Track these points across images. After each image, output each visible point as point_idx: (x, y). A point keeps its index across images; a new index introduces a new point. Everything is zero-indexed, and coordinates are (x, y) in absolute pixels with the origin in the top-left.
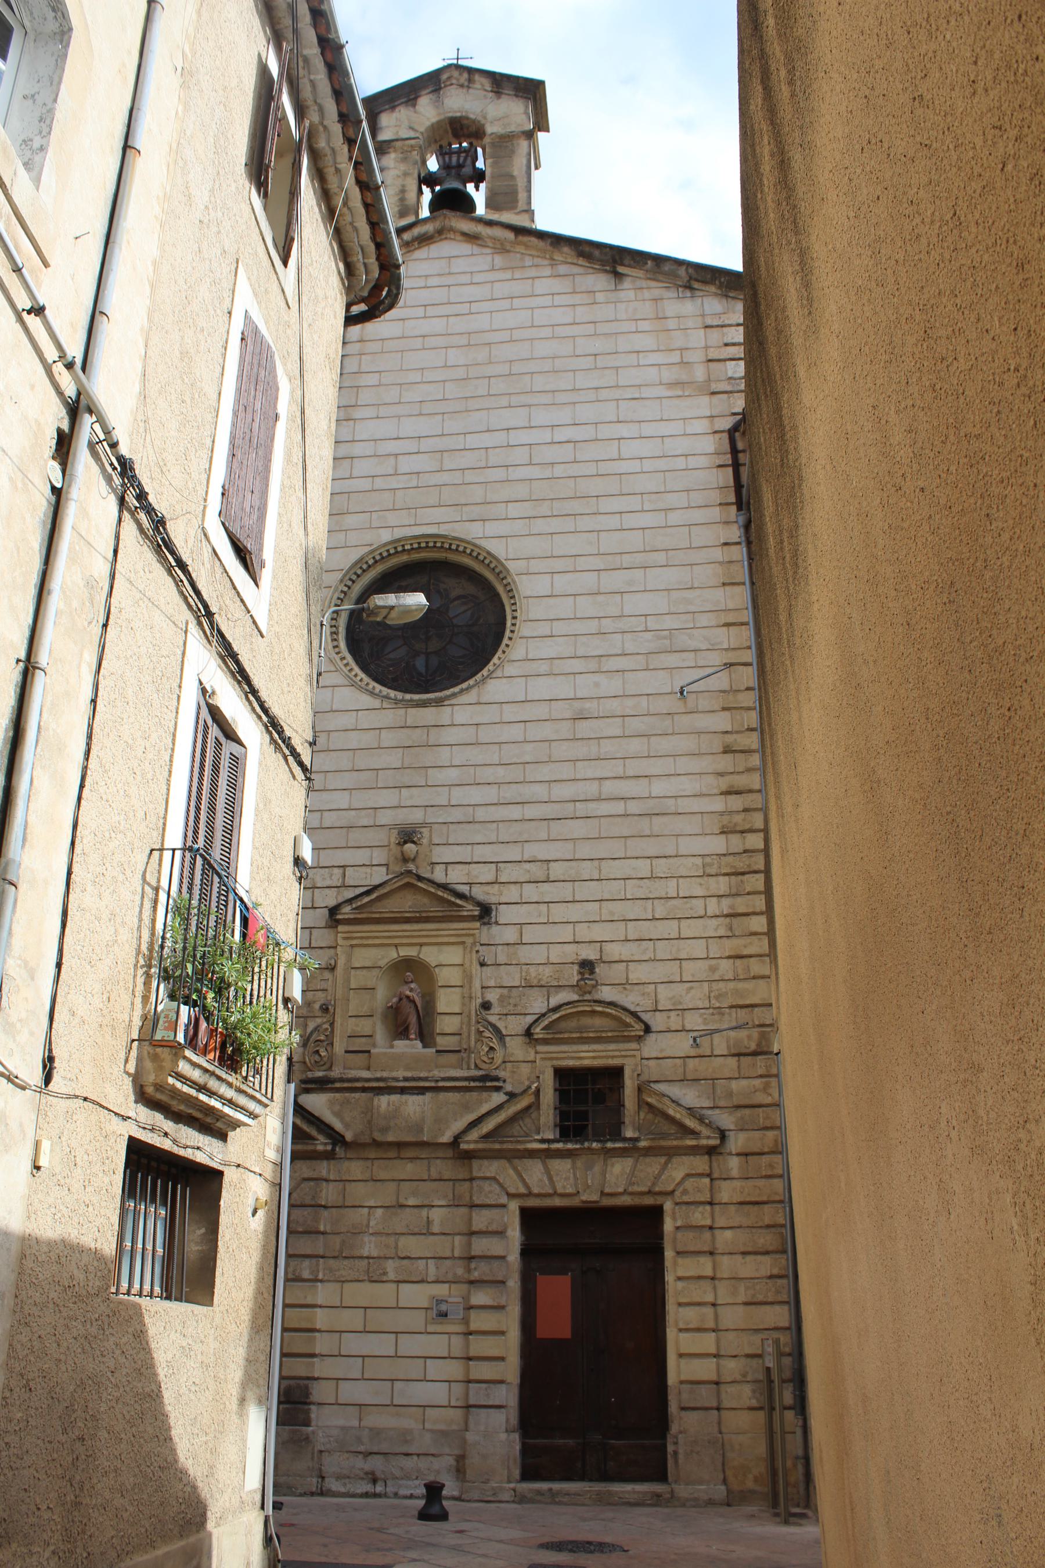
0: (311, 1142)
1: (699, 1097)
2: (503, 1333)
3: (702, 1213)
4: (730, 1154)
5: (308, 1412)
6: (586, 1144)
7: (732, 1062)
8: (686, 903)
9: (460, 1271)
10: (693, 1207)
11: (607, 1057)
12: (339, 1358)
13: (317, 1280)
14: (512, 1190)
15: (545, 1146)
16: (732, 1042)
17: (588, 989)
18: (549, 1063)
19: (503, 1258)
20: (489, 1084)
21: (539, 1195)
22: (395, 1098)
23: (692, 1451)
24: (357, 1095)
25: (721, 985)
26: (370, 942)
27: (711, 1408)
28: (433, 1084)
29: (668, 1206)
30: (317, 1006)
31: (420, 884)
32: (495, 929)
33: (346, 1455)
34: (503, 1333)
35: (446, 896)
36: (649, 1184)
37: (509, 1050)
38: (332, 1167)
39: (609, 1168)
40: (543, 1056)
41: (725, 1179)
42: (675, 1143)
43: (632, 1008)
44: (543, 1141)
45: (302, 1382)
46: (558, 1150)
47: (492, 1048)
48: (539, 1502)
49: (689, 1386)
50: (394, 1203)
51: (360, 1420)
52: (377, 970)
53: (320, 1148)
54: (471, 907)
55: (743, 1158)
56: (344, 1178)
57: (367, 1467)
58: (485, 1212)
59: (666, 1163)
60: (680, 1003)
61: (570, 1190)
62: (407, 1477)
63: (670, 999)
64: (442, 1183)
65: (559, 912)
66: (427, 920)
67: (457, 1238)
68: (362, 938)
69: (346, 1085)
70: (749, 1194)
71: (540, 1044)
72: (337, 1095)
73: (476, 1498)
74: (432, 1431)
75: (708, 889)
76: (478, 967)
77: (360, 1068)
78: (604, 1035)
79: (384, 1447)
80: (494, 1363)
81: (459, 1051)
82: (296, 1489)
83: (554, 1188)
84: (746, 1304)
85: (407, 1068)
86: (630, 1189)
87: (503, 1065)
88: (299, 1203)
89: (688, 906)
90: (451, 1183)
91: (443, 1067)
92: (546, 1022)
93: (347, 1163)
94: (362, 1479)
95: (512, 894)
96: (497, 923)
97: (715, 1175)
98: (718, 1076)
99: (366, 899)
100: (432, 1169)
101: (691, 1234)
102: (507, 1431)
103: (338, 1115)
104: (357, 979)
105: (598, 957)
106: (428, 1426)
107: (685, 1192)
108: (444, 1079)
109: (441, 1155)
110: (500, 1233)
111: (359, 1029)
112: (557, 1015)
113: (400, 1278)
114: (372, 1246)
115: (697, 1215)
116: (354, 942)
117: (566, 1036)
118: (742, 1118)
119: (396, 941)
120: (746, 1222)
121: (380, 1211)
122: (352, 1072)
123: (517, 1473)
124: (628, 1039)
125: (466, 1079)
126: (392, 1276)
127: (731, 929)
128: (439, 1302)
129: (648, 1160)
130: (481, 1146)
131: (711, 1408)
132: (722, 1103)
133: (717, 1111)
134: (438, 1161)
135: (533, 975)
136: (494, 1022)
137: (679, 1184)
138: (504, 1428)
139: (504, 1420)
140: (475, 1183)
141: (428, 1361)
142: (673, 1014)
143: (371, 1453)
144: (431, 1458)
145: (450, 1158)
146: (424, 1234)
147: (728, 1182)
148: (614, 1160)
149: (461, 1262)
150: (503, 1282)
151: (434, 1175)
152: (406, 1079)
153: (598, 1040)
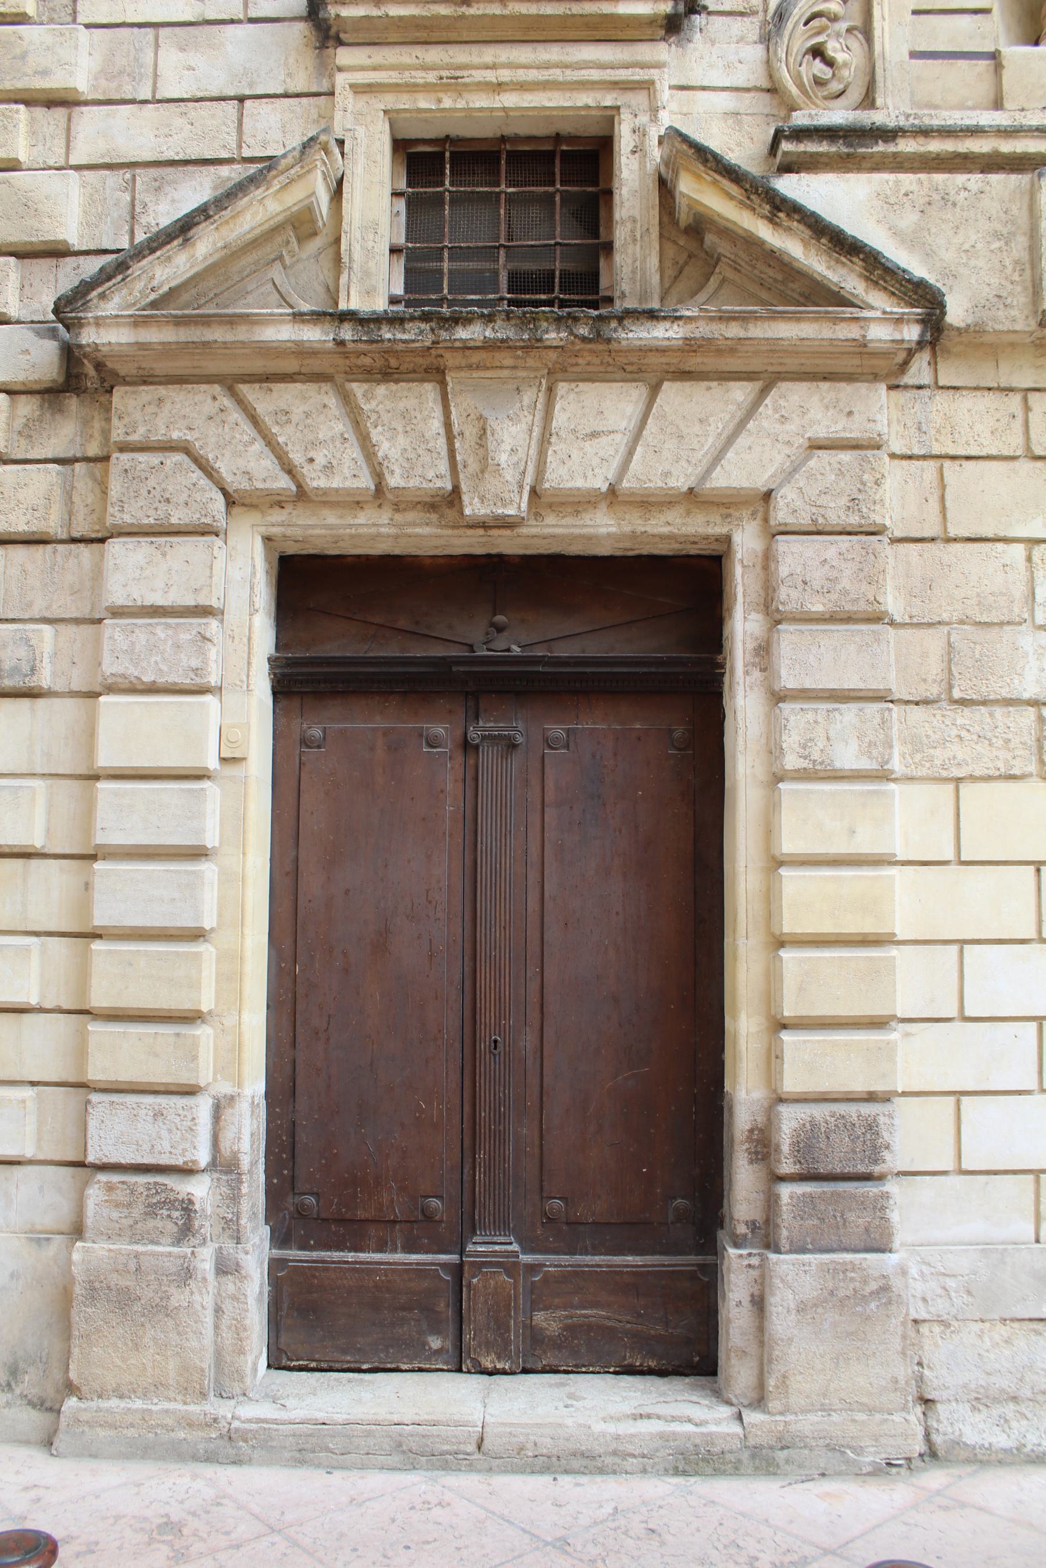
5: (880, 1206)
12: (958, 1025)
13: (883, 776)
24: (974, 180)
33: (1004, 1331)
45: (851, 1110)
53: (880, 333)
56: (936, 450)
69: (935, 146)
72: (908, 180)
82: (859, 1450)
88: (804, 520)
103: (912, 241)
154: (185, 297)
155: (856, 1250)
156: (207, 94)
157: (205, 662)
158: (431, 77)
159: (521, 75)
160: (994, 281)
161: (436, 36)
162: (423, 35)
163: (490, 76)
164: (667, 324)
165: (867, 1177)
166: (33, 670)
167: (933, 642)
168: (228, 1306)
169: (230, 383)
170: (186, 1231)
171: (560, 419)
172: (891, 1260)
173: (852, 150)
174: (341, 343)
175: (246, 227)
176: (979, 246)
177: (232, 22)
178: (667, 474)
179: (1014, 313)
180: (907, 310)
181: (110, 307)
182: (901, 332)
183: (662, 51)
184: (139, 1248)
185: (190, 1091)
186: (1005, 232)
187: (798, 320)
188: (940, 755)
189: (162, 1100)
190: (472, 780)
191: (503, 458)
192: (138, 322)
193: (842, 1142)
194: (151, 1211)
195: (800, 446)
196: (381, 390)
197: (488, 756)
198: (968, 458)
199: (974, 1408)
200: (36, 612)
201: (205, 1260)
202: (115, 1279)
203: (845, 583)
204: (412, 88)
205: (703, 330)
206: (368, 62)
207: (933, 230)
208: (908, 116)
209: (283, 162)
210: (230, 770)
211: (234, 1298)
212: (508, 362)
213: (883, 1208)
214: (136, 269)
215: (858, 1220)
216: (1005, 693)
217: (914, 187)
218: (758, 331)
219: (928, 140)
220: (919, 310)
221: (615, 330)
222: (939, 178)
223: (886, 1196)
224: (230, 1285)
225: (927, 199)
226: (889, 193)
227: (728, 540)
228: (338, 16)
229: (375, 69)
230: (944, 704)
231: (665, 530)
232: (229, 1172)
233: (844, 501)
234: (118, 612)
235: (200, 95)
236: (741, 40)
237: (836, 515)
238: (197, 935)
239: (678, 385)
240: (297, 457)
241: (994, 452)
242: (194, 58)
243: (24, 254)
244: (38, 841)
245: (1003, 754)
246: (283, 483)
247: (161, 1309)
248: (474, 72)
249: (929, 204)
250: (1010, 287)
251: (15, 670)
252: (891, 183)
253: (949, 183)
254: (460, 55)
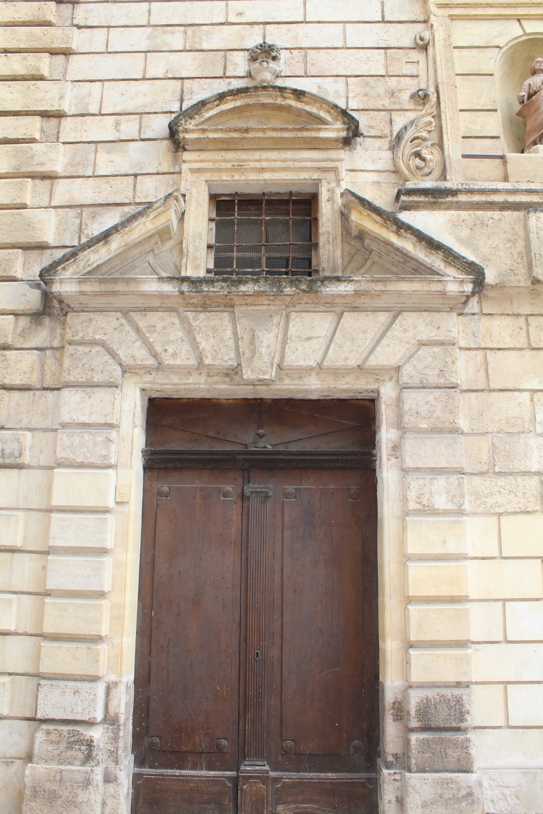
0: (436, 277)
5: (465, 746)
12: (504, 646)
13: (461, 512)
24: (497, 214)
30: (406, 96)
53: (453, 288)
56: (483, 345)
69: (476, 198)
72: (464, 214)
88: (416, 382)
103: (466, 243)
154: (105, 269)
155: (453, 771)
156: (119, 173)
157: (109, 452)
158: (229, 165)
159: (273, 165)
160: (509, 262)
161: (231, 147)
162: (225, 146)
163: (258, 165)
164: (346, 284)
165: (458, 729)
166: (20, 454)
167: (484, 444)
168: (109, 801)
169: (125, 313)
170: (88, 758)
171: (292, 330)
172: (473, 777)
173: (436, 200)
174: (182, 293)
175: (136, 236)
176: (500, 245)
177: (133, 140)
178: (346, 359)
179: (519, 277)
180: (466, 277)
181: (67, 274)
182: (463, 287)
183: (342, 154)
184: (62, 767)
185: (94, 679)
186: (512, 239)
187: (412, 281)
188: (490, 501)
189: (79, 684)
190: (245, 515)
191: (263, 350)
192: (81, 281)
193: (443, 710)
194: (70, 746)
195: (414, 344)
196: (202, 316)
197: (254, 503)
198: (499, 349)
200: (23, 425)
201: (98, 776)
202: (49, 786)
203: (438, 413)
204: (220, 170)
205: (364, 286)
206: (198, 158)
207: (477, 238)
208: (462, 184)
209: (155, 206)
210: (120, 508)
211: (114, 797)
212: (266, 302)
213: (467, 747)
214: (81, 256)
215: (454, 754)
216: (522, 469)
217: (467, 218)
218: (392, 287)
219: (473, 195)
220: (472, 277)
221: (320, 287)
222: (479, 213)
223: (468, 740)
224: (111, 788)
225: (474, 223)
226: (454, 220)
227: (378, 392)
228: (184, 138)
229: (201, 161)
231: (346, 387)
232: (113, 724)
233: (436, 372)
234: (64, 426)
235: (116, 173)
236: (380, 149)
237: (433, 378)
238: (101, 595)
239: (351, 314)
240: (159, 349)
241: (512, 346)
242: (114, 157)
243: (26, 248)
244: (19, 543)
246: (151, 362)
247: (72, 803)
248: (249, 163)
249: (475, 225)
250: (516, 265)
251: (11, 455)
252: (455, 216)
253: (484, 216)
254: (243, 155)
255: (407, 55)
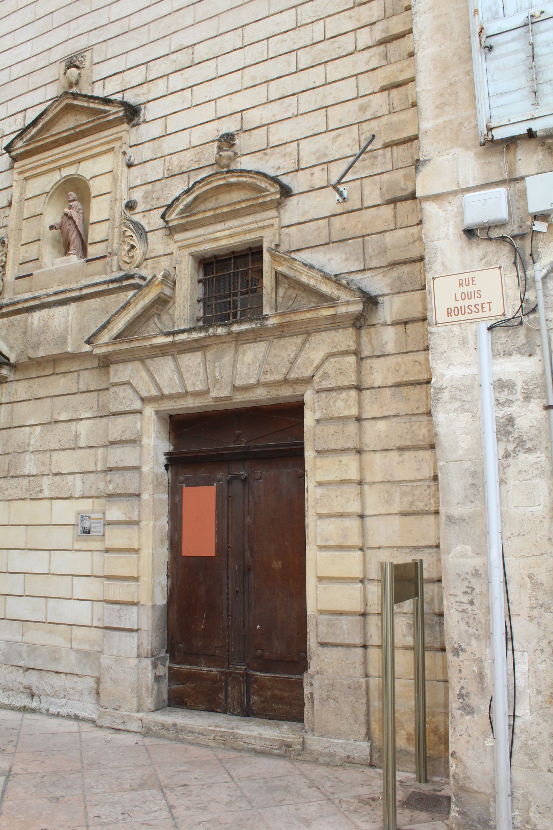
1: (346, 259)
2: (137, 551)
3: (346, 401)
4: (385, 324)
6: (211, 331)
7: (387, 211)
8: (333, 43)
9: (102, 486)
10: (334, 394)
11: (245, 233)
14: (144, 394)
15: (170, 339)
16: (385, 188)
17: (225, 162)
18: (187, 251)
19: (137, 468)
20: (125, 283)
21: (171, 397)
22: (44, 312)
23: (328, 697)
25: (374, 123)
26: (39, 170)
27: (355, 646)
28: (77, 294)
29: (309, 397)
31: (76, 102)
32: (143, 127)
33: (11, 669)
34: (137, 551)
35: (96, 106)
36: (285, 371)
37: (151, 246)
38: (4, 390)
39: (240, 358)
40: (179, 244)
41: (378, 357)
42: (309, 315)
43: (272, 173)
44: (168, 334)
46: (183, 343)
47: (133, 247)
48: (162, 737)
49: (328, 617)
50: (49, 420)
51: (23, 635)
52: (44, 196)
54: (117, 109)
55: (401, 328)
57: (26, 682)
58: (120, 420)
59: (304, 343)
60: (325, 155)
61: (200, 387)
62: (55, 695)
63: (314, 153)
64: (88, 394)
65: (201, 93)
66: (83, 134)
67: (100, 450)
68: (32, 169)
70: (407, 373)
71: (176, 232)
73: (107, 725)
74: (77, 651)
75: (358, 20)
76: (125, 169)
77: (26, 292)
78: (238, 207)
79: (38, 664)
80: (126, 583)
81: (105, 257)
83: (184, 385)
84: (403, 514)
85: (61, 283)
86: (263, 380)
87: (145, 263)
89: (336, 45)
90: (96, 393)
91: (91, 275)
92: (181, 207)
93: (15, 385)
94: (22, 692)
95: (159, 88)
96: (145, 122)
97: (365, 353)
98: (369, 232)
99: (34, 131)
100: (81, 382)
101: (331, 428)
102: (138, 656)
104: (30, 209)
105: (239, 128)
106: (75, 645)
107: (326, 376)
108: (86, 287)
109: (88, 366)
110: (135, 441)
111: (28, 255)
112: (191, 197)
113: (53, 495)
114: (32, 463)
115: (340, 404)
116: (27, 175)
117: (200, 216)
118: (399, 278)
119: (59, 164)
120: (403, 408)
121: (38, 428)
122: (19, 296)
123: (149, 702)
124: (264, 207)
125: (105, 282)
126: (46, 493)
127: (386, 57)
128: (84, 518)
129: (282, 342)
130: (111, 348)
131: (355, 646)
132: (374, 263)
133: (368, 274)
134: (86, 372)
135: (175, 163)
136: (138, 221)
137: (318, 368)
138: (135, 653)
139: (135, 646)
140: (112, 390)
141: (75, 578)
142: (317, 170)
143: (29, 669)
144: (75, 678)
145: (97, 368)
146: (74, 449)
147: (382, 359)
148: (245, 346)
149: (102, 476)
150: (139, 495)
151: (83, 388)
152: (56, 293)
153: (234, 214)
160: (21, 347)
199: (3, 692)
216: (22, 473)
217: (6, 322)
230: (9, 478)
245: (21, 492)
255: (4, 212)
